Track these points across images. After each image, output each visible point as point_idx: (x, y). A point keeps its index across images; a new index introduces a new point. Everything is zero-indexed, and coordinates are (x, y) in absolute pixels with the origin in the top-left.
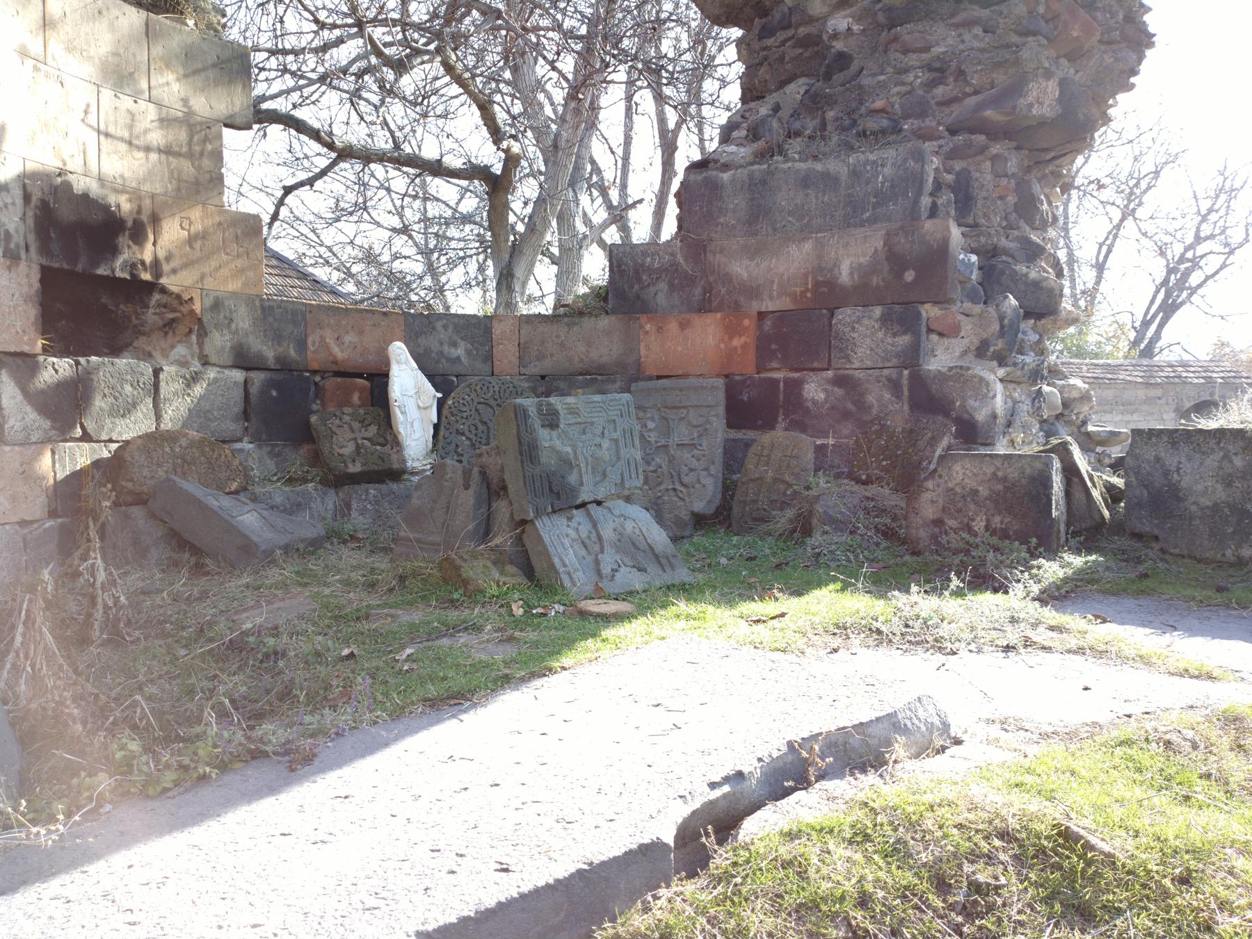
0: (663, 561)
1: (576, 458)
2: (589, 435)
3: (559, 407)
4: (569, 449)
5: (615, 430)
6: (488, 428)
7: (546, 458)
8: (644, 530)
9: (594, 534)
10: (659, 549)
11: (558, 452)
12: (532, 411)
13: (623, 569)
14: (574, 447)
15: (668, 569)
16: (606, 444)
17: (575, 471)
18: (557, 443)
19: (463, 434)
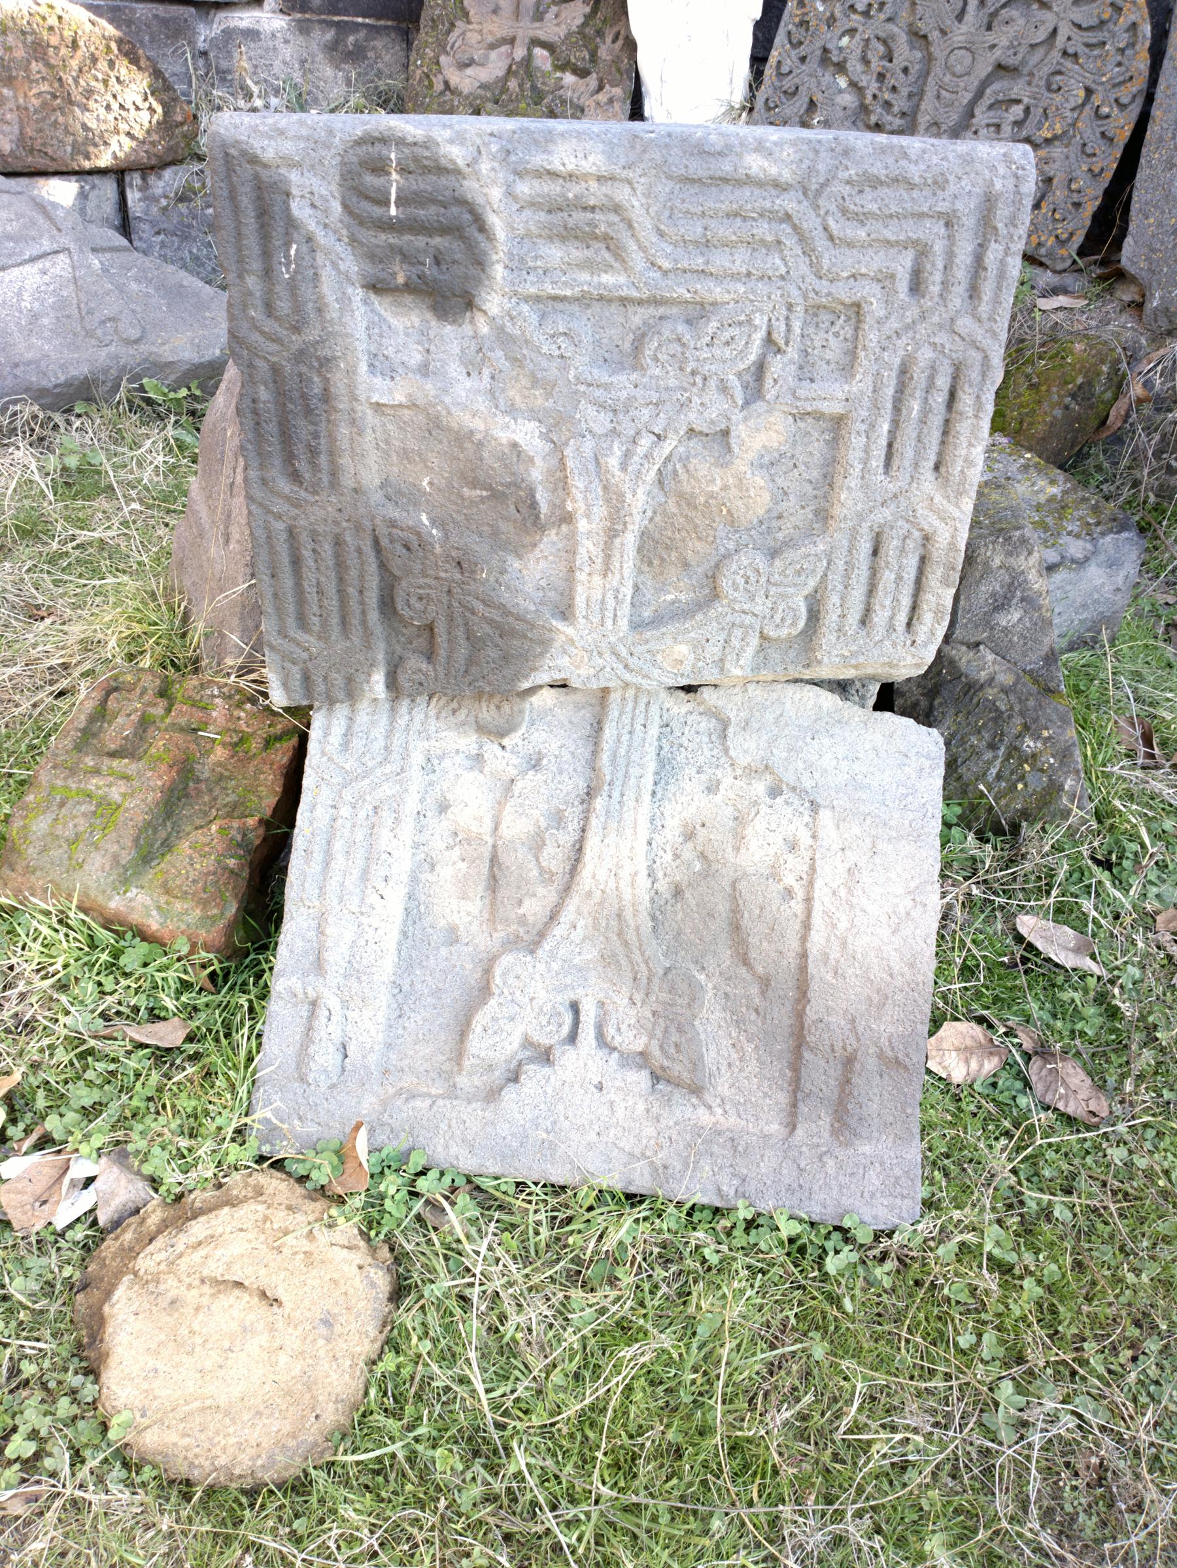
0: (821, 1075)
1: (560, 481)
2: (660, 373)
3: (490, 190)
4: (527, 434)
5: (847, 368)
6: (929, 58)
7: (368, 460)
8: (830, 874)
9: (568, 837)
10: (835, 1003)
11: (462, 438)
12: (315, 201)
13: (582, 1062)
14: (558, 427)
15: (816, 1126)
16: (762, 433)
17: (551, 540)
18: (466, 399)
19: (841, 68)
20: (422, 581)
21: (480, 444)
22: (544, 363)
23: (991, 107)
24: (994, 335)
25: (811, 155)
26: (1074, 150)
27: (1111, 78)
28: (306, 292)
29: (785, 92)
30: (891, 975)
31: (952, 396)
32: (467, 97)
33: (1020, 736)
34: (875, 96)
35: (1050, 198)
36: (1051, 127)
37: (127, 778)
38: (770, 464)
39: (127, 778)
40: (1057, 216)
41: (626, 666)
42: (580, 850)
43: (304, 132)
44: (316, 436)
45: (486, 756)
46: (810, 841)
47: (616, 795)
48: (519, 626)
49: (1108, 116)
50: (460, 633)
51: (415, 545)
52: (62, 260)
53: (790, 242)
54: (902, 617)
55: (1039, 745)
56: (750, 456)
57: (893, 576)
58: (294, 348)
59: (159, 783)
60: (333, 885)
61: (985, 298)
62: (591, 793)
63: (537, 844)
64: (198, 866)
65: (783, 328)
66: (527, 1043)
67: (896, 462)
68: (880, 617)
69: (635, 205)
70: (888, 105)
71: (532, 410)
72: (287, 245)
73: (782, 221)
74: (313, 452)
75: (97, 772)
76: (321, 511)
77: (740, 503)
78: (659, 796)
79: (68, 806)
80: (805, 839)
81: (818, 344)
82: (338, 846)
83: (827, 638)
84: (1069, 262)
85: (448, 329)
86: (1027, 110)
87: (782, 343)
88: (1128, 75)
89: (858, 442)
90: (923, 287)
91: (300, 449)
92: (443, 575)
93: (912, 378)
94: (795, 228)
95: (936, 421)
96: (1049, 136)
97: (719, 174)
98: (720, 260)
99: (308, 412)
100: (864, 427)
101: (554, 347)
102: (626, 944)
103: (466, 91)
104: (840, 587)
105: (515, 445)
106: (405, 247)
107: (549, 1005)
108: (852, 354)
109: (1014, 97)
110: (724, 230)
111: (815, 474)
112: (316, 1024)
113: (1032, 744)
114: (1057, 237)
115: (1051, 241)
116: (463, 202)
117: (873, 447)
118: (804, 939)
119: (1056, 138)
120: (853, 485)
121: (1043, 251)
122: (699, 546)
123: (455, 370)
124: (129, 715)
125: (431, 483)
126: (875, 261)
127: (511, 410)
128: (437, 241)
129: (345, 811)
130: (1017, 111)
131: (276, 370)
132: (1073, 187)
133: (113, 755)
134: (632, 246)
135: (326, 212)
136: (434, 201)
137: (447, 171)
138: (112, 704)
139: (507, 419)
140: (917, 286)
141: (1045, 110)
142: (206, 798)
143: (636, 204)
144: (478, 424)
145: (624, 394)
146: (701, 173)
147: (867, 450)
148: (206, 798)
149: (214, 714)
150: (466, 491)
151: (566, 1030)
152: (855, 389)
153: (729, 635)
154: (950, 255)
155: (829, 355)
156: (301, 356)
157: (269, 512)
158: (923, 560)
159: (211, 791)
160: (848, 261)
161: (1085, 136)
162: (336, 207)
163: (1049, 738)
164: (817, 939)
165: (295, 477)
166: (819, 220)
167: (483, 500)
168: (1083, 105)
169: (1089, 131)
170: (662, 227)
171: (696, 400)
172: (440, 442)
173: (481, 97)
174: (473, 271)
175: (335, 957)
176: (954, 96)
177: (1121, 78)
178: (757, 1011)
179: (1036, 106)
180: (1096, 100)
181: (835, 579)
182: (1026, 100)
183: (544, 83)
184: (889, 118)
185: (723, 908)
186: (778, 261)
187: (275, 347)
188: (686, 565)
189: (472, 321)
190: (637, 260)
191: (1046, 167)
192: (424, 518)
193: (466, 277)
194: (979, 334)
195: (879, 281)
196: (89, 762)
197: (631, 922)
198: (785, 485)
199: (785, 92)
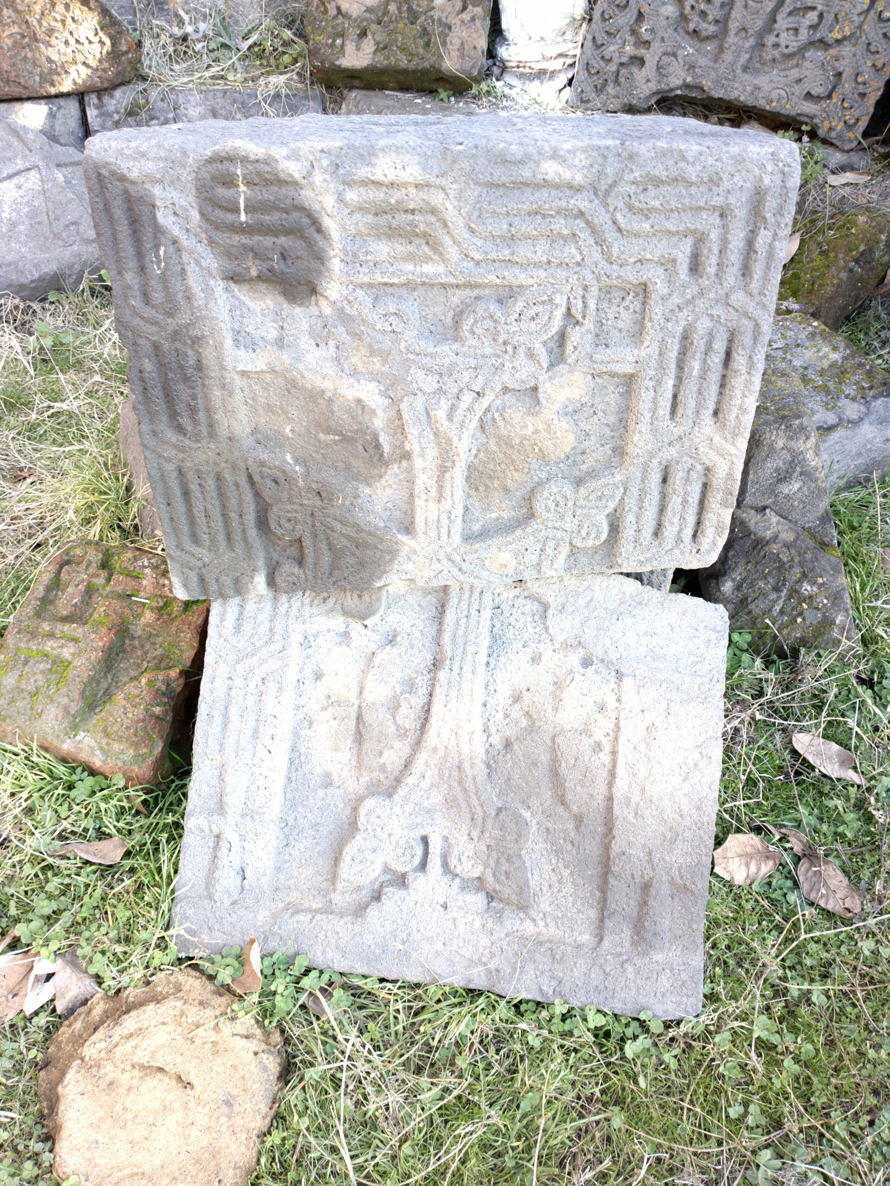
0: (623, 899)
1: (399, 428)
2: (476, 341)
3: (324, 198)
4: (369, 393)
5: (637, 334)
8: (632, 732)
9: (418, 700)
10: (634, 838)
11: (315, 396)
13: (430, 886)
14: (394, 388)
15: (619, 937)
16: (566, 388)
18: (317, 366)
20: (289, 507)
21: (330, 400)
22: (379, 337)
23: (790, 14)
24: (764, 307)
25: (600, 160)
26: (860, 49)
28: (176, 285)
29: (618, 6)
30: (681, 816)
31: (728, 354)
32: (356, 20)
33: (799, 581)
34: (693, 7)
35: (840, 90)
36: (841, 30)
37: (75, 640)
38: (573, 412)
39: (75, 640)
40: (846, 105)
41: (460, 570)
42: (428, 710)
43: (163, 154)
44: (194, 397)
45: (352, 634)
46: (616, 704)
47: (456, 668)
48: (370, 540)
50: (323, 546)
51: (281, 480)
52: (33, 175)
53: (584, 234)
54: (688, 532)
55: (815, 589)
56: (557, 406)
57: (680, 500)
58: (170, 329)
59: (101, 644)
60: (230, 743)
61: (756, 277)
62: (436, 665)
63: (394, 707)
64: (130, 715)
65: (580, 305)
66: (387, 869)
67: (680, 410)
68: (670, 532)
69: (449, 207)
70: (703, 14)
71: (372, 373)
72: (157, 247)
73: (576, 217)
74: (193, 410)
75: (51, 636)
76: (203, 455)
77: (549, 443)
78: (492, 666)
79: (30, 664)
80: (611, 702)
81: (611, 316)
82: (234, 711)
83: (626, 548)
84: (855, 143)
85: (298, 310)
86: (821, 16)
87: (579, 317)
89: (646, 396)
90: (700, 268)
91: (181, 408)
92: (306, 502)
93: (692, 343)
94: (588, 222)
95: (714, 378)
96: (839, 37)
97: (520, 179)
98: (524, 252)
99: (186, 379)
100: (651, 384)
101: (387, 324)
102: (465, 791)
103: (354, 15)
104: (635, 509)
105: (359, 401)
106: (256, 247)
107: (404, 840)
108: (640, 325)
109: (809, 5)
110: (526, 227)
111: (612, 419)
112: (219, 854)
113: (809, 588)
114: (845, 122)
116: (301, 209)
117: (660, 399)
118: (610, 785)
119: (845, 38)
120: (643, 430)
121: (833, 134)
122: (517, 475)
123: (306, 342)
124: (77, 585)
125: (292, 431)
126: (659, 249)
127: (355, 373)
128: (282, 240)
129: (239, 682)
130: (813, 16)
131: (156, 347)
132: (860, 79)
133: (65, 620)
134: (448, 241)
135: (187, 219)
136: (277, 209)
137: (287, 183)
138: (64, 576)
139: (352, 380)
140: (695, 267)
141: (836, 15)
142: (139, 653)
143: (450, 206)
144: (328, 385)
145: (447, 361)
146: (504, 179)
147: (655, 402)
148: (139, 653)
149: (144, 582)
150: (322, 436)
151: (417, 860)
152: (643, 354)
153: (544, 545)
154: (724, 242)
155: (620, 324)
156: (176, 335)
157: (160, 456)
158: (705, 486)
159: (142, 646)
160: (633, 249)
161: (870, 37)
162: (195, 215)
163: (823, 584)
164: (621, 786)
165: (180, 429)
166: (608, 215)
167: (335, 442)
168: (868, 10)
169: (873, 32)
170: (473, 226)
171: (508, 364)
172: (298, 398)
173: (366, 19)
174: (314, 264)
175: (233, 801)
176: (759, 5)
178: (572, 842)
179: (829, 12)
181: (631, 502)
182: (820, 7)
183: (418, 5)
184: (705, 25)
185: (544, 758)
186: (574, 251)
187: (154, 329)
188: (506, 490)
189: (317, 304)
190: (453, 253)
191: (837, 64)
192: (289, 458)
193: (309, 270)
194: (751, 306)
195: (662, 264)
196: (46, 627)
197: (469, 772)
198: (587, 428)
199: (618, 6)
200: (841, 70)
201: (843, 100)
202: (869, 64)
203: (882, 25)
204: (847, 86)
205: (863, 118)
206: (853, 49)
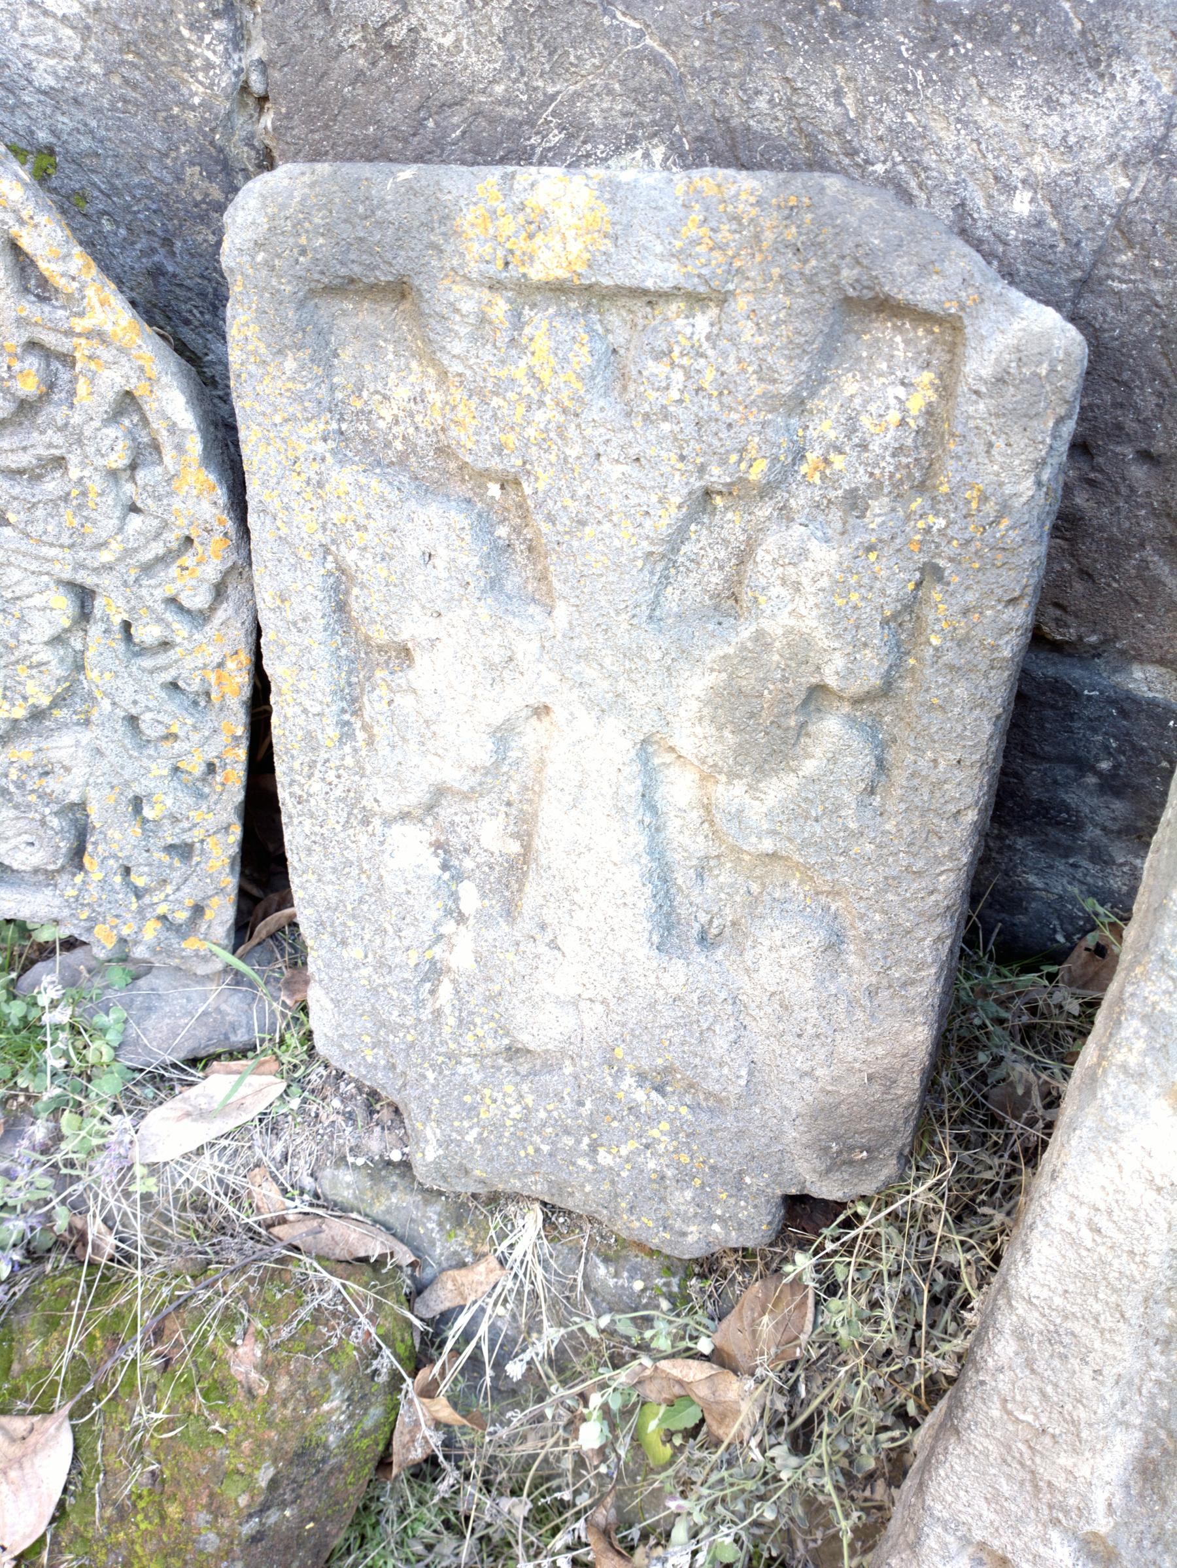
26: (108, 735)
27: (128, 552)
49: (165, 645)
88: (172, 538)
115: (151, 931)
177: (158, 548)
180: (111, 606)
200: (74, 797)
201: (127, 871)
202: (161, 769)
203: (147, 663)
204: (115, 837)
205: (215, 902)
206: (86, 736)
